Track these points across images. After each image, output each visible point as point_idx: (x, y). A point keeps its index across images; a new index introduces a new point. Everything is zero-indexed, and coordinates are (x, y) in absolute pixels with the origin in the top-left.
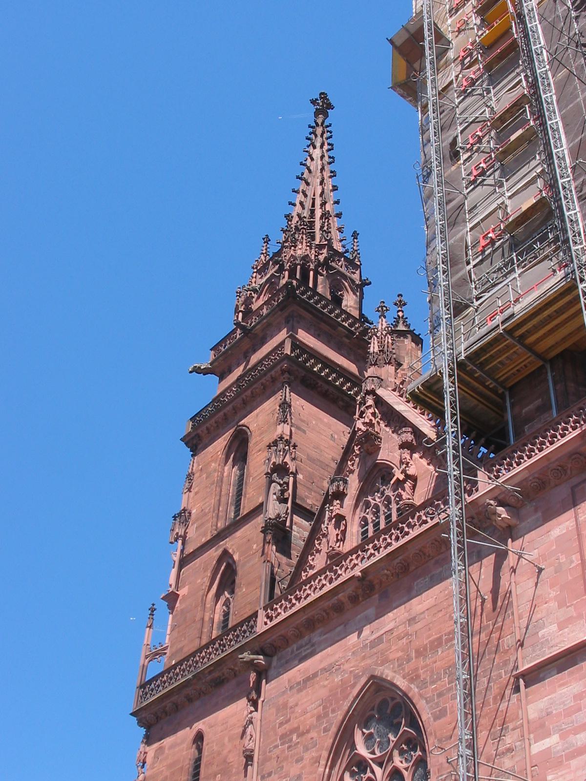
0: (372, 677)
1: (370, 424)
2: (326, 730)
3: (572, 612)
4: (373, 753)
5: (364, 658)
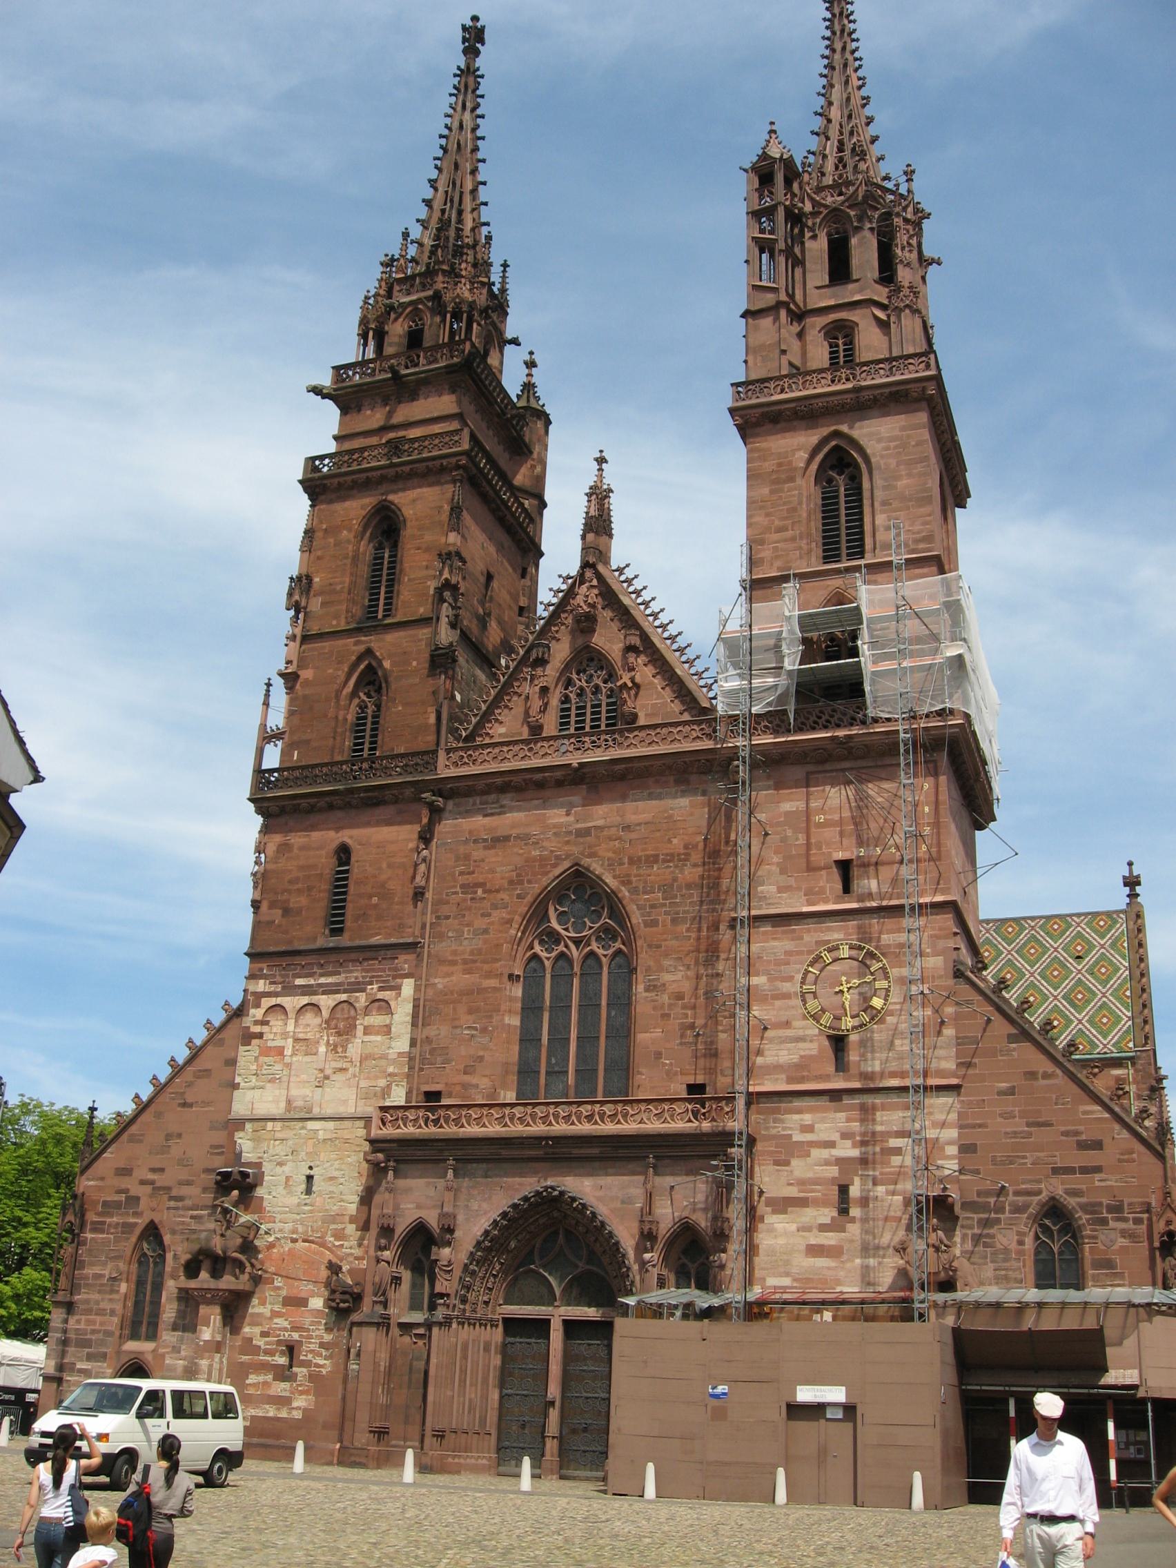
0: (577, 864)
1: (593, 606)
2: (519, 896)
3: (792, 881)
4: (566, 930)
5: (567, 843)
